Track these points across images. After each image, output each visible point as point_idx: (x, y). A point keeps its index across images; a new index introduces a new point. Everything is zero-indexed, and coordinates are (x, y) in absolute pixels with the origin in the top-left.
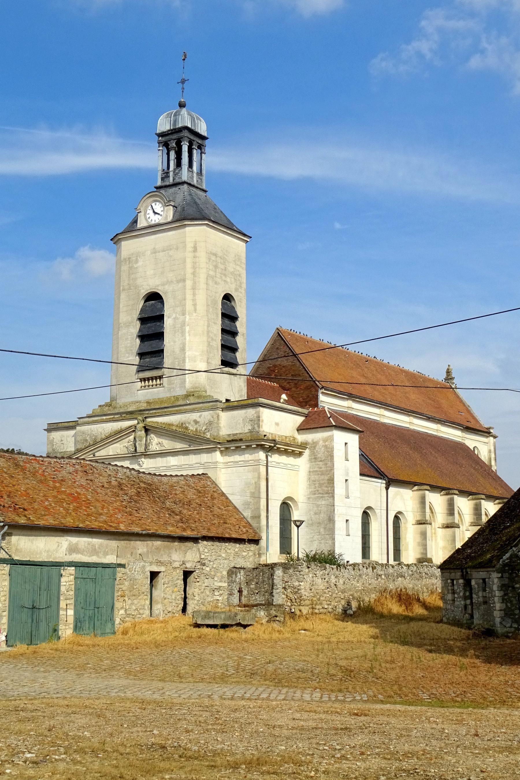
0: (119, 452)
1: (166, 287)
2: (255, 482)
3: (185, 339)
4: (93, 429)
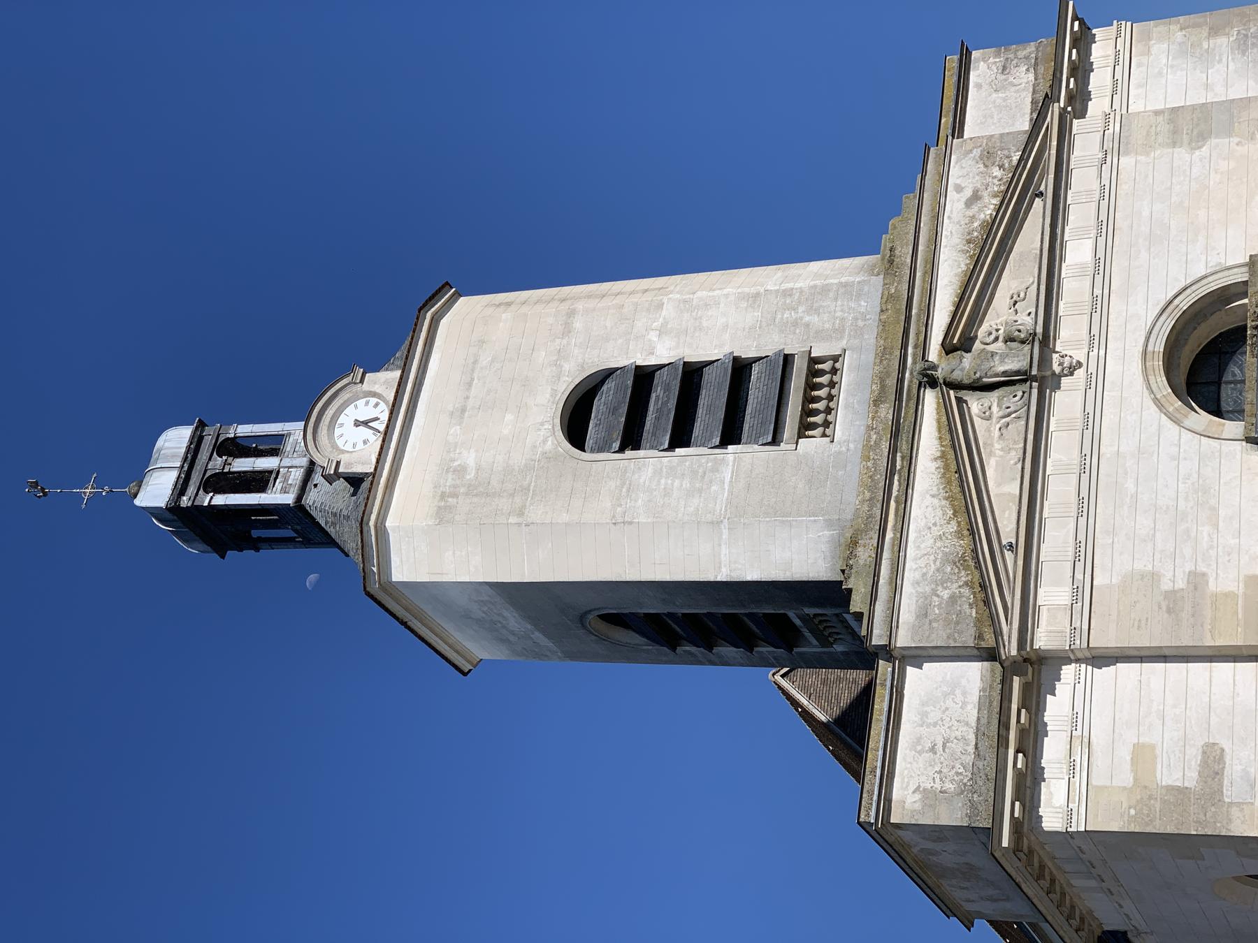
0: (1015, 455)
1: (566, 367)
2: (1181, 29)
3: (727, 296)
4: (918, 575)
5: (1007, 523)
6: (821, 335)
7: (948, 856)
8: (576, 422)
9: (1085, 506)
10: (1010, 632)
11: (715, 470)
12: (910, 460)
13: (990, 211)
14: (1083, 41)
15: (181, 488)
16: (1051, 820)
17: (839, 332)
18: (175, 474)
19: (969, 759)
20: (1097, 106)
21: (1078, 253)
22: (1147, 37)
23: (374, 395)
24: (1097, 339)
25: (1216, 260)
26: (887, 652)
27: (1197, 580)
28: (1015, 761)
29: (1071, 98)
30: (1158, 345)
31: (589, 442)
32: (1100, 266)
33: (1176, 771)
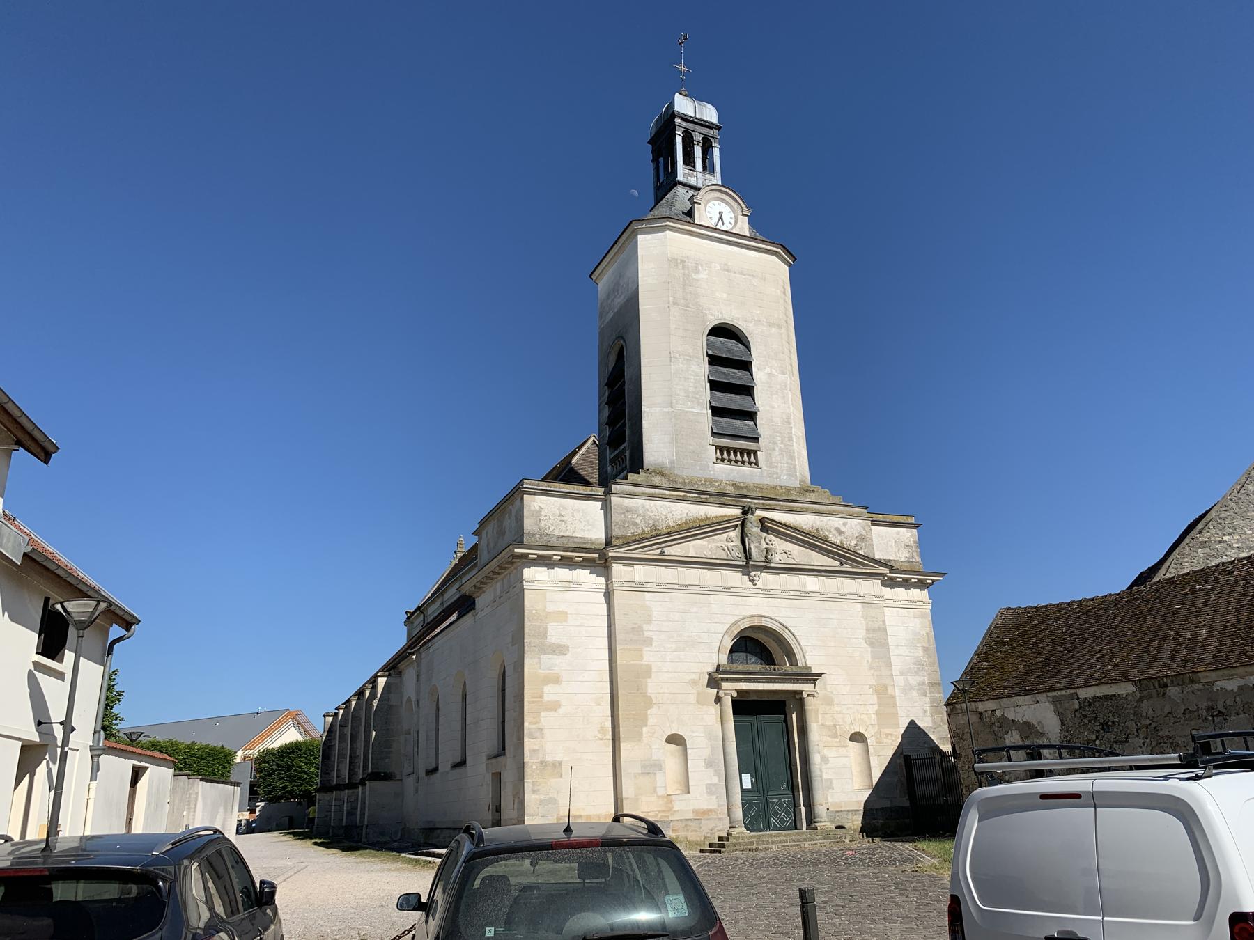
0: (709, 554)
5: (675, 551)
6: (769, 456)
7: (508, 523)
8: (722, 331)
9: (684, 588)
10: (620, 552)
11: (699, 404)
12: (705, 502)
13: (833, 540)
14: (921, 585)
15: (685, 118)
16: (529, 573)
17: (770, 465)
18: (692, 114)
19: (557, 533)
20: (887, 591)
21: (811, 583)
22: (922, 616)
23: (736, 222)
24: (768, 593)
25: (808, 650)
26: (608, 492)
27: (649, 642)
28: (557, 555)
29: (891, 579)
30: (765, 623)
31: (712, 338)
32: (805, 594)
33: (555, 633)
